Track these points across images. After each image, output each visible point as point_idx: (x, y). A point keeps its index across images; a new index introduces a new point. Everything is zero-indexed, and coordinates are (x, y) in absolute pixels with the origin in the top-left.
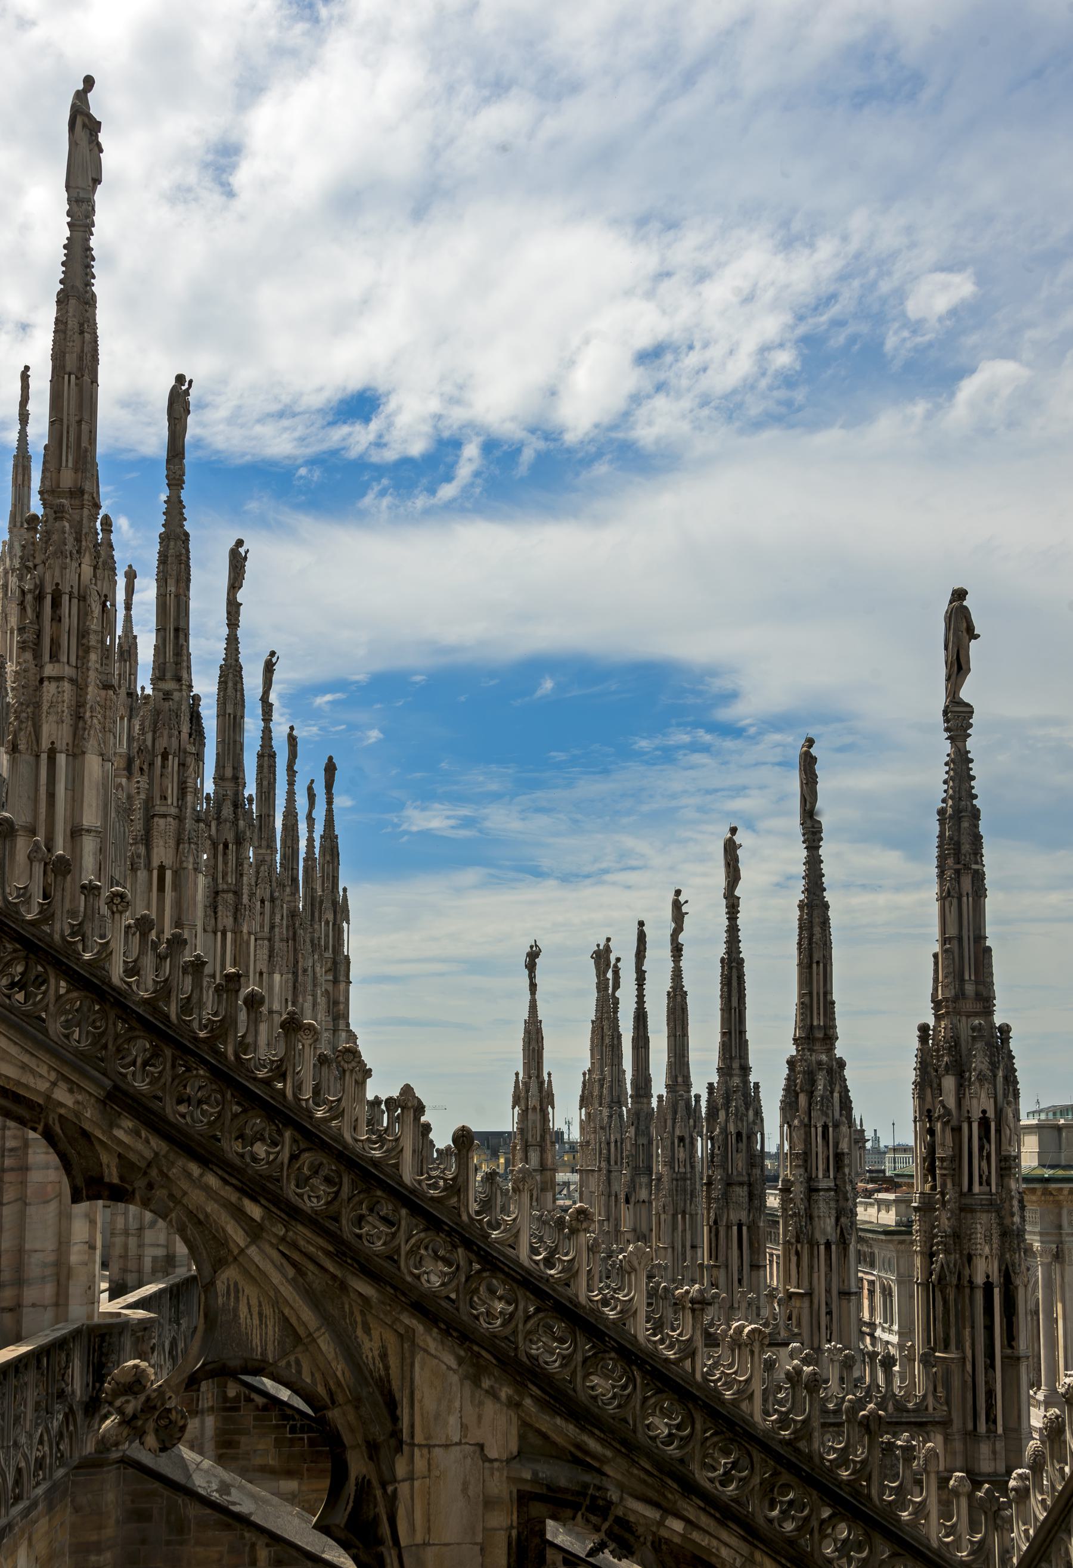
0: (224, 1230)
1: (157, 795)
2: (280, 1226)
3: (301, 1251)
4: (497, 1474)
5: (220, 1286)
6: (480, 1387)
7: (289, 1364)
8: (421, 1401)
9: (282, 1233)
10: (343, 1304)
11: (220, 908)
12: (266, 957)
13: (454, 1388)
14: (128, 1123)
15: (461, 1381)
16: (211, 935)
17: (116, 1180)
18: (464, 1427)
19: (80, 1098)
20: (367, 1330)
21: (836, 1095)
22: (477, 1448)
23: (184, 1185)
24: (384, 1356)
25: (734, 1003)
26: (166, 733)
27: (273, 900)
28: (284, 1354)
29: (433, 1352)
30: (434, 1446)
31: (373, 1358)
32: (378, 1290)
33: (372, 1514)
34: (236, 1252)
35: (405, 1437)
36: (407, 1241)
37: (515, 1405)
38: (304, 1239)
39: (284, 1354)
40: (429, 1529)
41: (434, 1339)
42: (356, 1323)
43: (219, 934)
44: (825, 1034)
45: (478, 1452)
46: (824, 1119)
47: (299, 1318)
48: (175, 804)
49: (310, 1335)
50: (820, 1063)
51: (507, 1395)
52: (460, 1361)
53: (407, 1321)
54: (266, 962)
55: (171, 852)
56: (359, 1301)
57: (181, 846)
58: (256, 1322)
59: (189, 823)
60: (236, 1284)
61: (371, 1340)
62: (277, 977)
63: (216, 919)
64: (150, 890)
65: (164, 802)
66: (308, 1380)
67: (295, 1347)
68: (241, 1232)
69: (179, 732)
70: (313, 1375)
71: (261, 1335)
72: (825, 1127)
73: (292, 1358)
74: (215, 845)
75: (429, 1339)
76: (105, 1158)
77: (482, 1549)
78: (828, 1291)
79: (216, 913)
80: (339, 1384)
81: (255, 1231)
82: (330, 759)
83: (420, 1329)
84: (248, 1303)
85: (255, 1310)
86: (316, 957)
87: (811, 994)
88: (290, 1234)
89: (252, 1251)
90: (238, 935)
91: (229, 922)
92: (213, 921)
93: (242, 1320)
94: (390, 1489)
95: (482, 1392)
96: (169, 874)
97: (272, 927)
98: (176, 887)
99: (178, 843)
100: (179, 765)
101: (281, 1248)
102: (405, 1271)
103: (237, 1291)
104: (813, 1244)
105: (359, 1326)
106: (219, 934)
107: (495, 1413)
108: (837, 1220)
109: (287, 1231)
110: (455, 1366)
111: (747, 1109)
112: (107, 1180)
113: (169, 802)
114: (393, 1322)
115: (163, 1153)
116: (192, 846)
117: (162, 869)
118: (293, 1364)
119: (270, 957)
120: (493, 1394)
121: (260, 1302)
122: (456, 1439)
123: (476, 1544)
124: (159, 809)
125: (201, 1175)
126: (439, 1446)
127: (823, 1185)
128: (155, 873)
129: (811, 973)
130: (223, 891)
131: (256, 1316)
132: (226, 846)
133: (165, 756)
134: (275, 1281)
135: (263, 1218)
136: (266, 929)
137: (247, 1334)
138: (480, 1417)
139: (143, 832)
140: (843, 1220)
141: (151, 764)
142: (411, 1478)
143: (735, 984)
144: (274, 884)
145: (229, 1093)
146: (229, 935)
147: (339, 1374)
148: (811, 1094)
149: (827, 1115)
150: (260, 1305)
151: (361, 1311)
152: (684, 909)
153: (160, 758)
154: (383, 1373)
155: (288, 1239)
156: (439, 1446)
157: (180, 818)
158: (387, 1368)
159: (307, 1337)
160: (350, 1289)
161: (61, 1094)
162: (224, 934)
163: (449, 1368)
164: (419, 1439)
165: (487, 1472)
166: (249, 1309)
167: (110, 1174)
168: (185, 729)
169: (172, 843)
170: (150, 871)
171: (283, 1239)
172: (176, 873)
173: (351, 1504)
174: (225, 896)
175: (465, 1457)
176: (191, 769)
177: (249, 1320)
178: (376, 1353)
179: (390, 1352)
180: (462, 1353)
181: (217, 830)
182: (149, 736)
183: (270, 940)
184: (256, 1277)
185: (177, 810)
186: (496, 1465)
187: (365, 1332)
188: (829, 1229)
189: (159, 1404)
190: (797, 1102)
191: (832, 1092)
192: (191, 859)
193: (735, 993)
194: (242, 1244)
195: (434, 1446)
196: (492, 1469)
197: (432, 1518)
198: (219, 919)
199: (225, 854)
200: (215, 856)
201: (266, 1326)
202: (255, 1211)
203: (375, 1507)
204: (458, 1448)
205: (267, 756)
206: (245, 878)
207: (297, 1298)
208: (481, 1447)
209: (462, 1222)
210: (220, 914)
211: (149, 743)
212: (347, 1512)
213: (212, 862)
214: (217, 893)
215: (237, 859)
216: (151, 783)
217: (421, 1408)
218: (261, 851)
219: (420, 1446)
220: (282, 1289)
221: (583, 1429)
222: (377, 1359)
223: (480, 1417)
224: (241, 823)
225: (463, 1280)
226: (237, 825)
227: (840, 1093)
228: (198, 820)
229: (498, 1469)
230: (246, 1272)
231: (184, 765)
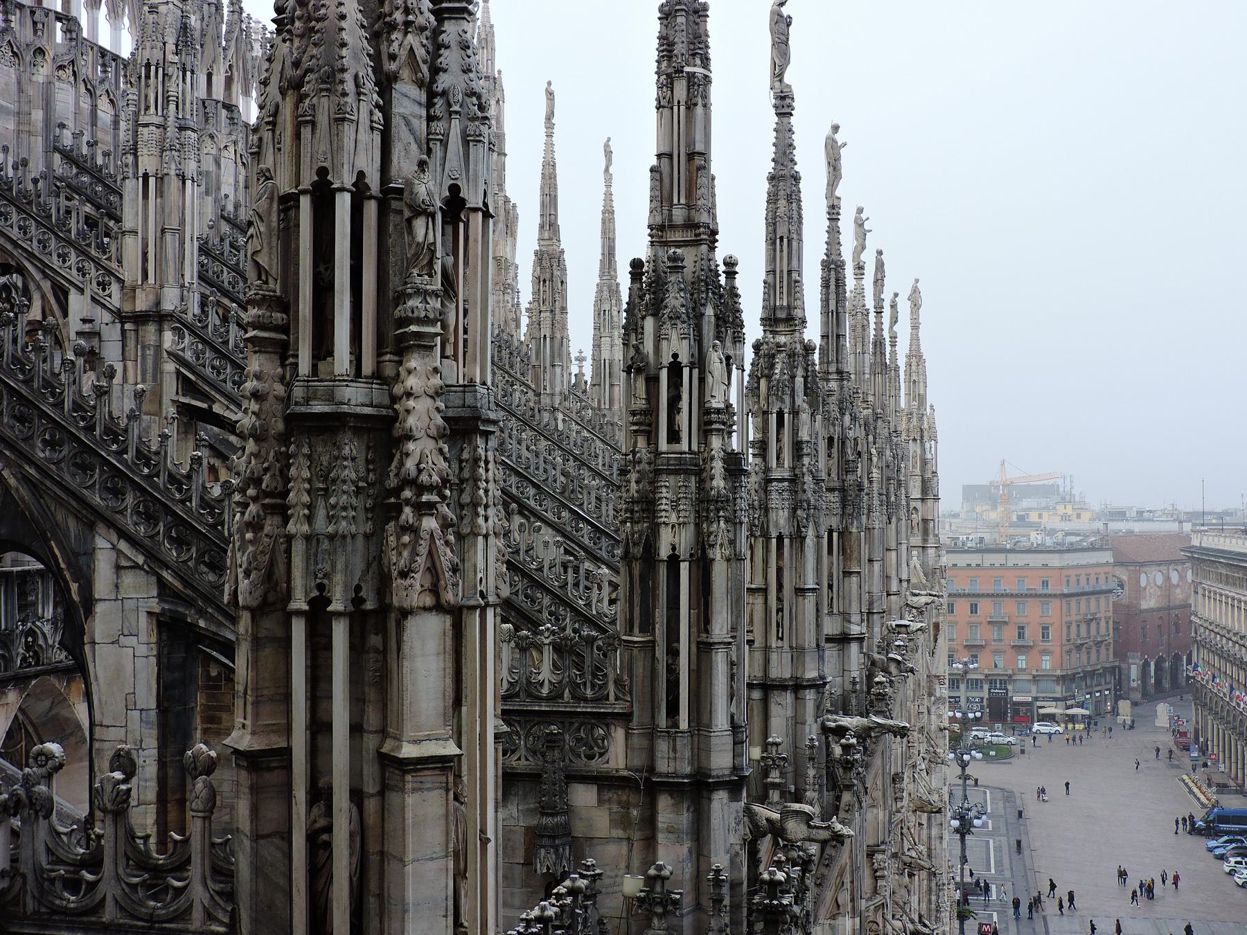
21: (799, 381)
25: (832, 306)
44: (789, 314)
46: (779, 404)
50: (778, 345)
72: (780, 415)
78: (780, 587)
87: (774, 271)
104: (766, 537)
108: (794, 510)
111: (843, 414)
124: (143, 119)
127: (776, 474)
129: (775, 250)
140: (799, 512)
143: (833, 287)
148: (769, 378)
149: (783, 401)
152: (867, 226)
188: (782, 522)
190: (758, 388)
191: (793, 377)
193: (832, 296)
227: (806, 378)
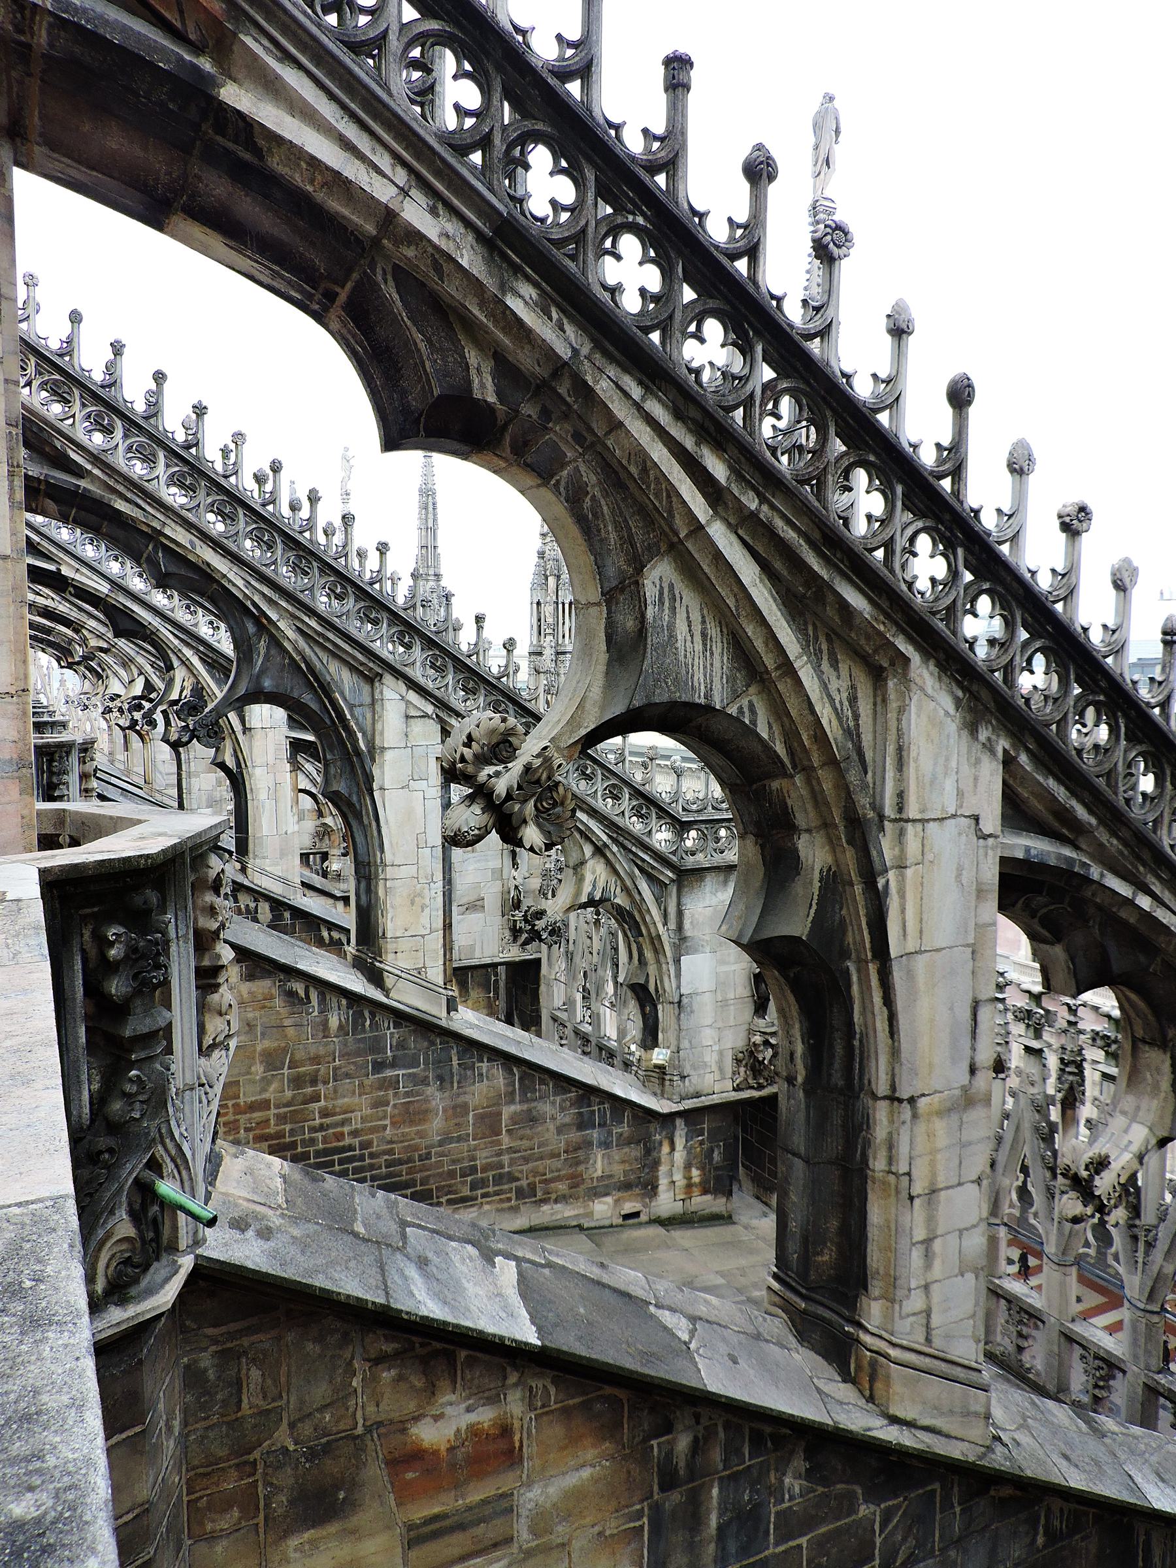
2: (751, 494)
4: (990, 852)
5: (650, 591)
6: (977, 739)
7: (740, 709)
8: (916, 760)
13: (952, 741)
14: (528, 291)
15: (960, 729)
17: (492, 398)
18: (960, 794)
20: (834, 664)
22: (973, 822)
24: (853, 700)
28: (736, 696)
29: (930, 691)
30: (928, 821)
31: (841, 703)
33: (837, 918)
35: (889, 811)
37: (1008, 762)
39: (736, 696)
40: (921, 932)
41: (932, 674)
42: (821, 651)
45: (973, 826)
51: (1005, 750)
52: (958, 703)
58: (699, 647)
60: (671, 586)
61: (838, 677)
66: (765, 735)
67: (748, 686)
70: (770, 727)
71: (705, 667)
73: (745, 702)
75: (926, 674)
76: (473, 357)
77: (973, 952)
80: (820, 735)
84: (688, 617)
85: (697, 629)
94: (881, 883)
95: (980, 746)
101: (740, 532)
103: (673, 599)
105: (825, 657)
107: (991, 775)
109: (760, 503)
110: (952, 711)
112: (477, 394)
118: (746, 710)
120: (989, 747)
121: (703, 617)
122: (952, 811)
123: (968, 945)
125: (643, 398)
126: (934, 820)
131: (698, 638)
137: (686, 665)
138: (976, 779)
142: (902, 867)
147: (825, 722)
150: (704, 622)
154: (851, 724)
155: (762, 516)
156: (934, 820)
158: (856, 717)
159: (777, 669)
160: (830, 598)
161: (415, 213)
163: (947, 713)
164: (912, 812)
165: (981, 851)
166: (689, 626)
167: (483, 386)
173: (814, 907)
175: (960, 834)
177: (689, 644)
178: (845, 695)
179: (859, 695)
180: (960, 694)
186: (991, 841)
187: (831, 666)
189: (544, 776)
194: (703, 520)
195: (928, 821)
196: (986, 847)
197: (925, 917)
201: (712, 654)
203: (841, 909)
204: (952, 821)
207: (774, 607)
208: (976, 819)
212: (810, 918)
217: (917, 770)
219: (914, 821)
221: (1073, 794)
222: (846, 703)
223: (976, 779)
229: (993, 848)
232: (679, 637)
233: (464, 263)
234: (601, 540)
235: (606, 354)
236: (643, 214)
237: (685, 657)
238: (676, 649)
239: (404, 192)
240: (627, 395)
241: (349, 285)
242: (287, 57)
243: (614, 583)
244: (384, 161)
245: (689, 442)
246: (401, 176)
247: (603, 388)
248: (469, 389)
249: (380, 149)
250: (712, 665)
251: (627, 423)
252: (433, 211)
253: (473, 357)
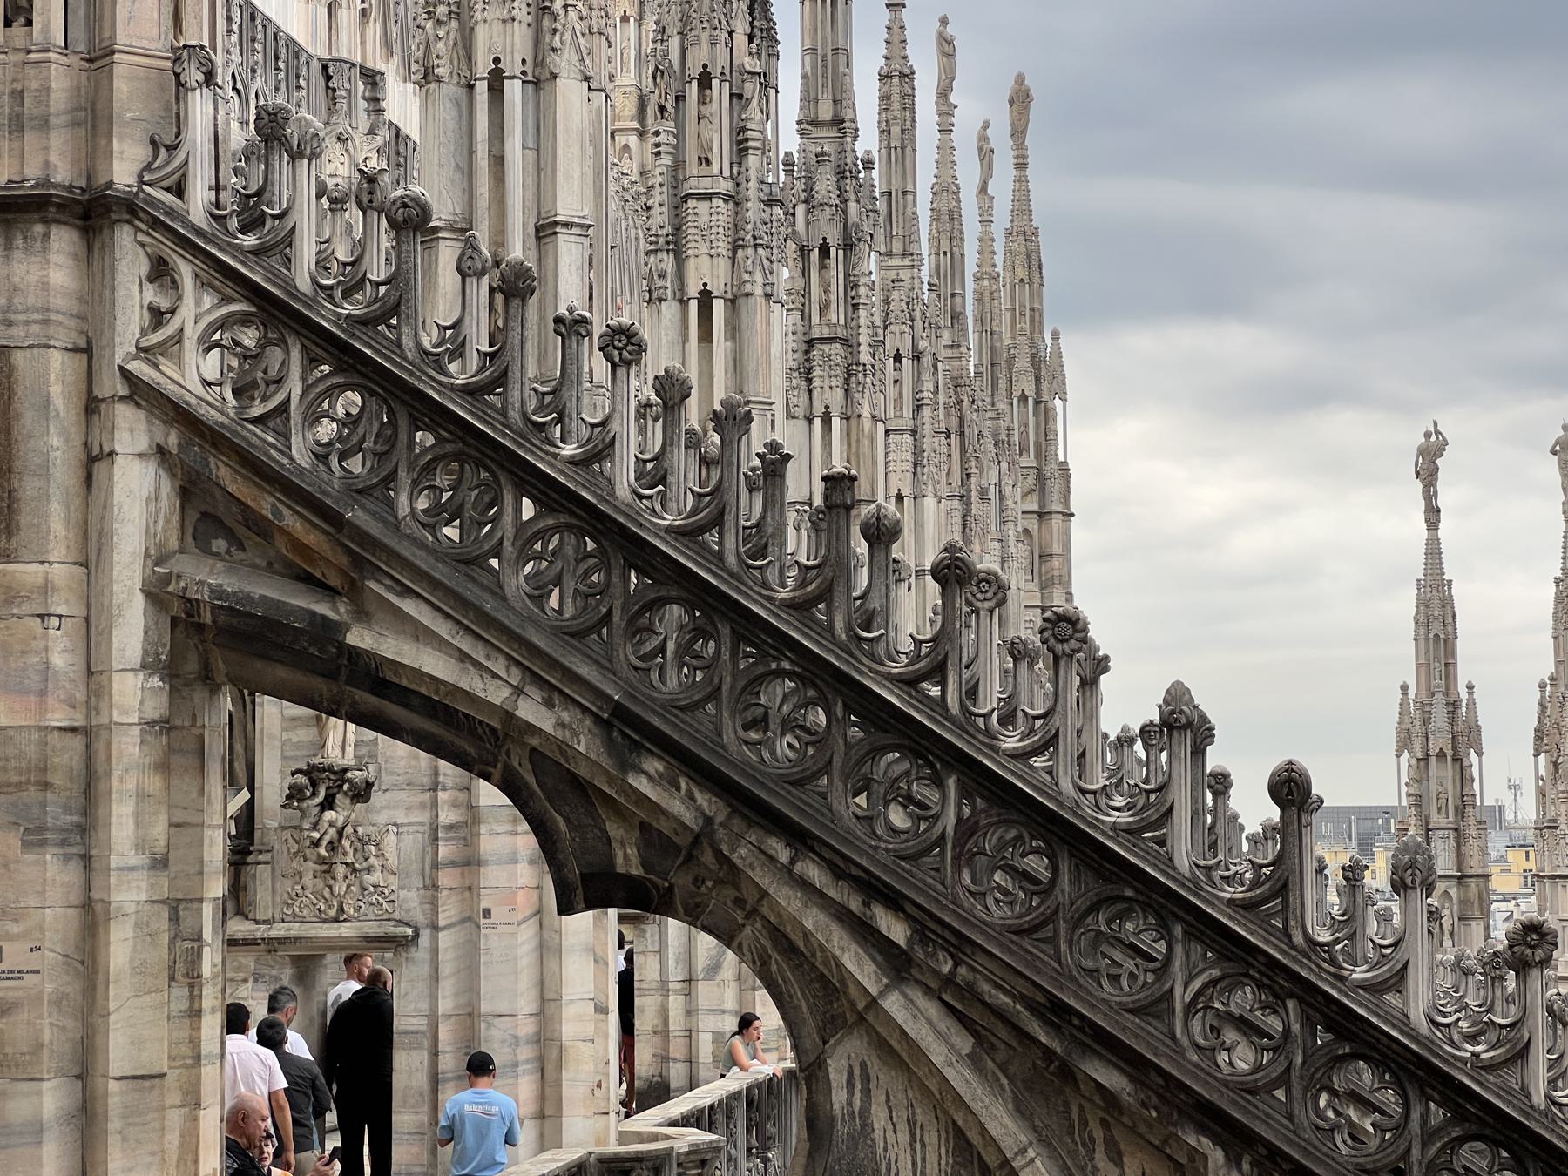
0: (839, 964)
1: (692, 156)
3: (984, 1003)
9: (946, 968)
10: (1067, 1104)
11: (817, 372)
12: (909, 466)
14: (654, 766)
16: (803, 424)
17: (636, 871)
19: (565, 716)
20: (1117, 1158)
23: (762, 877)
26: (705, 37)
27: (917, 357)
32: (1132, 1079)
34: (861, 1006)
36: (1186, 985)
38: (989, 980)
43: (817, 421)
47: (983, 1131)
48: (727, 173)
49: (1006, 1163)
53: (1191, 1140)
54: (909, 476)
55: (723, 265)
56: (1097, 1099)
57: (740, 253)
58: (904, 1137)
59: (753, 210)
62: (929, 503)
63: (810, 391)
64: (685, 339)
65: (704, 170)
68: (870, 967)
69: (730, 34)
74: (804, 251)
76: (614, 830)
79: (809, 381)
81: (898, 965)
82: (1020, 80)
83: (1216, 1156)
86: (1004, 465)
88: (962, 970)
89: (893, 1004)
90: (853, 421)
91: (836, 399)
92: (807, 396)
93: (878, 1134)
96: (719, 307)
97: (918, 408)
98: (734, 331)
99: (736, 246)
100: (731, 95)
101: (946, 997)
102: (1185, 1042)
103: (866, 1078)
106: (817, 421)
109: (956, 965)
112: (620, 870)
113: (716, 169)
114: (1165, 1142)
115: (720, 818)
116: (761, 251)
117: (706, 298)
119: (915, 466)
124: (693, 186)
125: (793, 861)
128: (693, 305)
130: (822, 340)
131: (903, 1128)
132: (824, 250)
133: (705, 80)
134: (937, 1060)
135: (909, 941)
136: (908, 412)
139: (668, 229)
141: (680, 99)
144: (919, 324)
145: (840, 704)
146: (836, 422)
151: (1103, 1120)
153: (695, 83)
155: (958, 980)
157: (735, 200)
161: (531, 711)
162: (826, 419)
168: (741, 27)
169: (724, 248)
170: (684, 302)
171: (949, 981)
172: (732, 302)
174: (826, 348)
176: (755, 102)
177: (890, 1134)
181: (808, 223)
182: (674, 44)
183: (914, 433)
184: (899, 1054)
185: (730, 184)
192: (759, 278)
194: (874, 991)
198: (816, 393)
199: (823, 267)
200: (805, 272)
202: (896, 930)
205: (897, 77)
206: (862, 313)
209: (1294, 947)
210: (816, 383)
211: (675, 56)
213: (800, 283)
214: (810, 343)
215: (847, 275)
216: (680, 135)
218: (891, 262)
220: (950, 1074)
224: (852, 206)
225: (1299, 1060)
226: (844, 211)
228: (770, 202)
230: (881, 1046)
231: (740, 96)
232: (876, 1126)
233: (582, 749)
234: (795, 1008)
235: (744, 817)
236: (788, 658)
237: (885, 1150)
238: (873, 1140)
239: (518, 691)
240: (772, 859)
241: (499, 766)
242: (407, 592)
243: (812, 1058)
244: (498, 666)
245: (855, 904)
246: (515, 677)
247: (741, 855)
248: (612, 865)
249: (494, 654)
250: (924, 1159)
251: (771, 891)
252: (549, 704)
253: (614, 830)
